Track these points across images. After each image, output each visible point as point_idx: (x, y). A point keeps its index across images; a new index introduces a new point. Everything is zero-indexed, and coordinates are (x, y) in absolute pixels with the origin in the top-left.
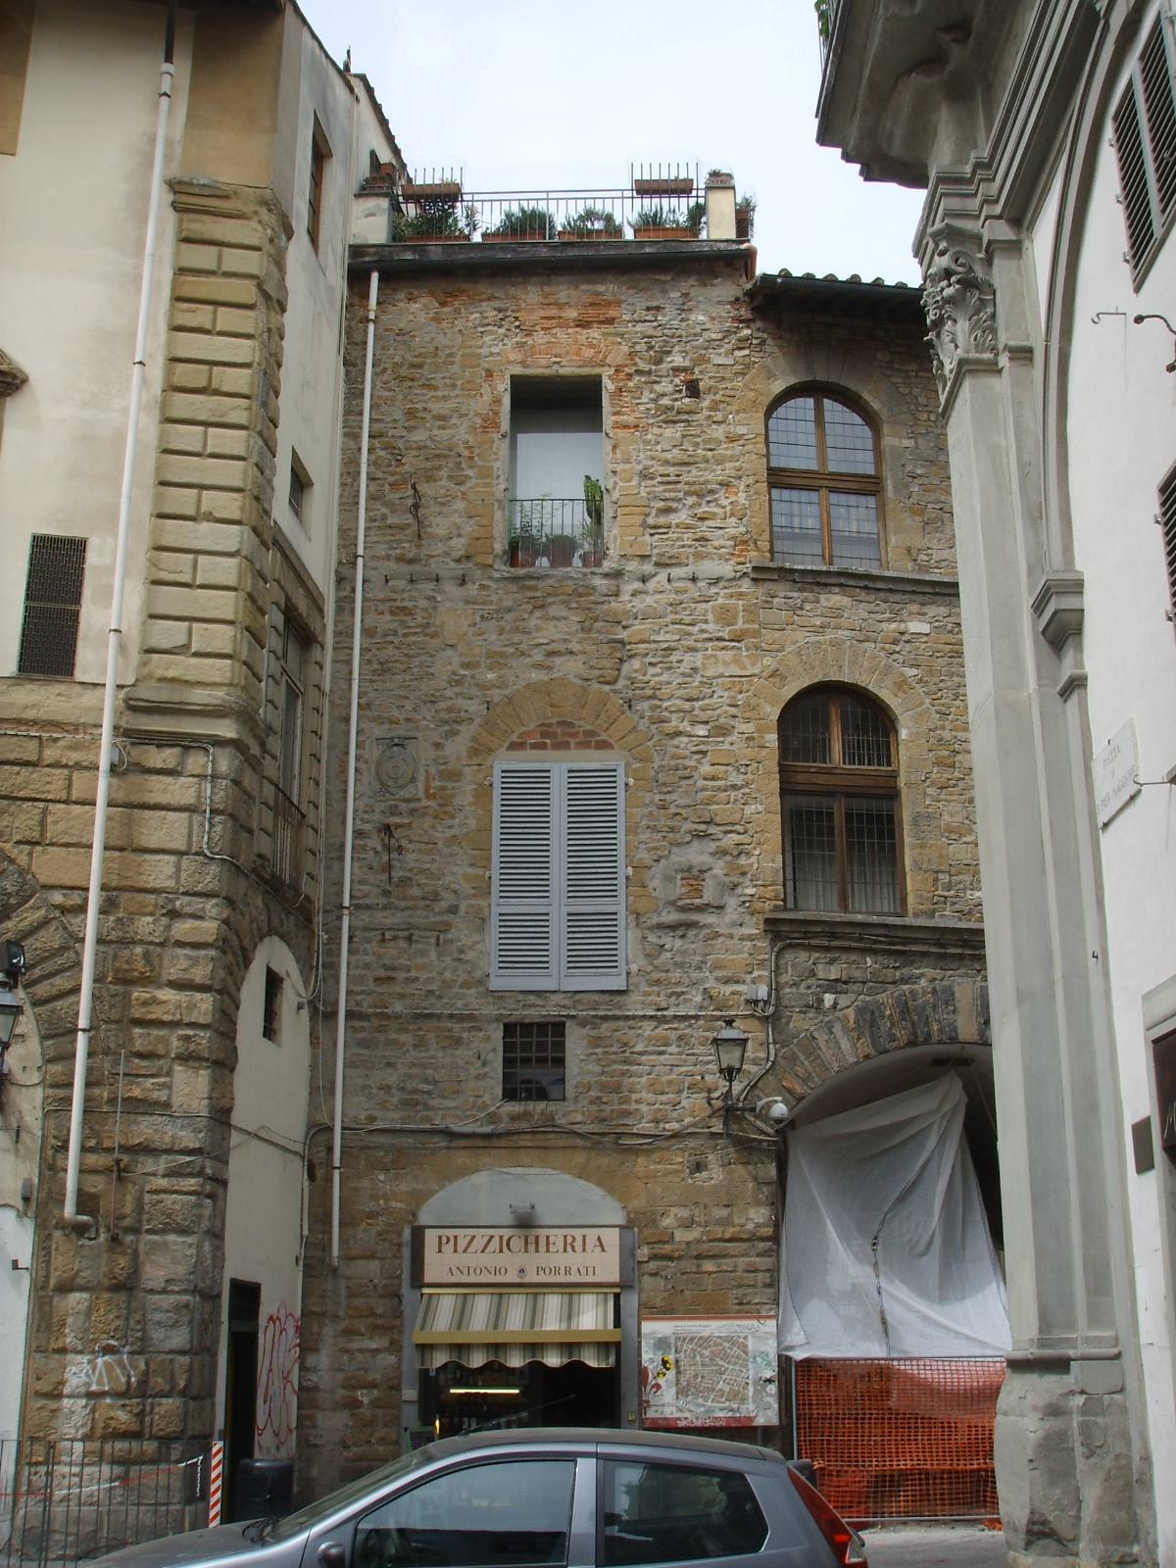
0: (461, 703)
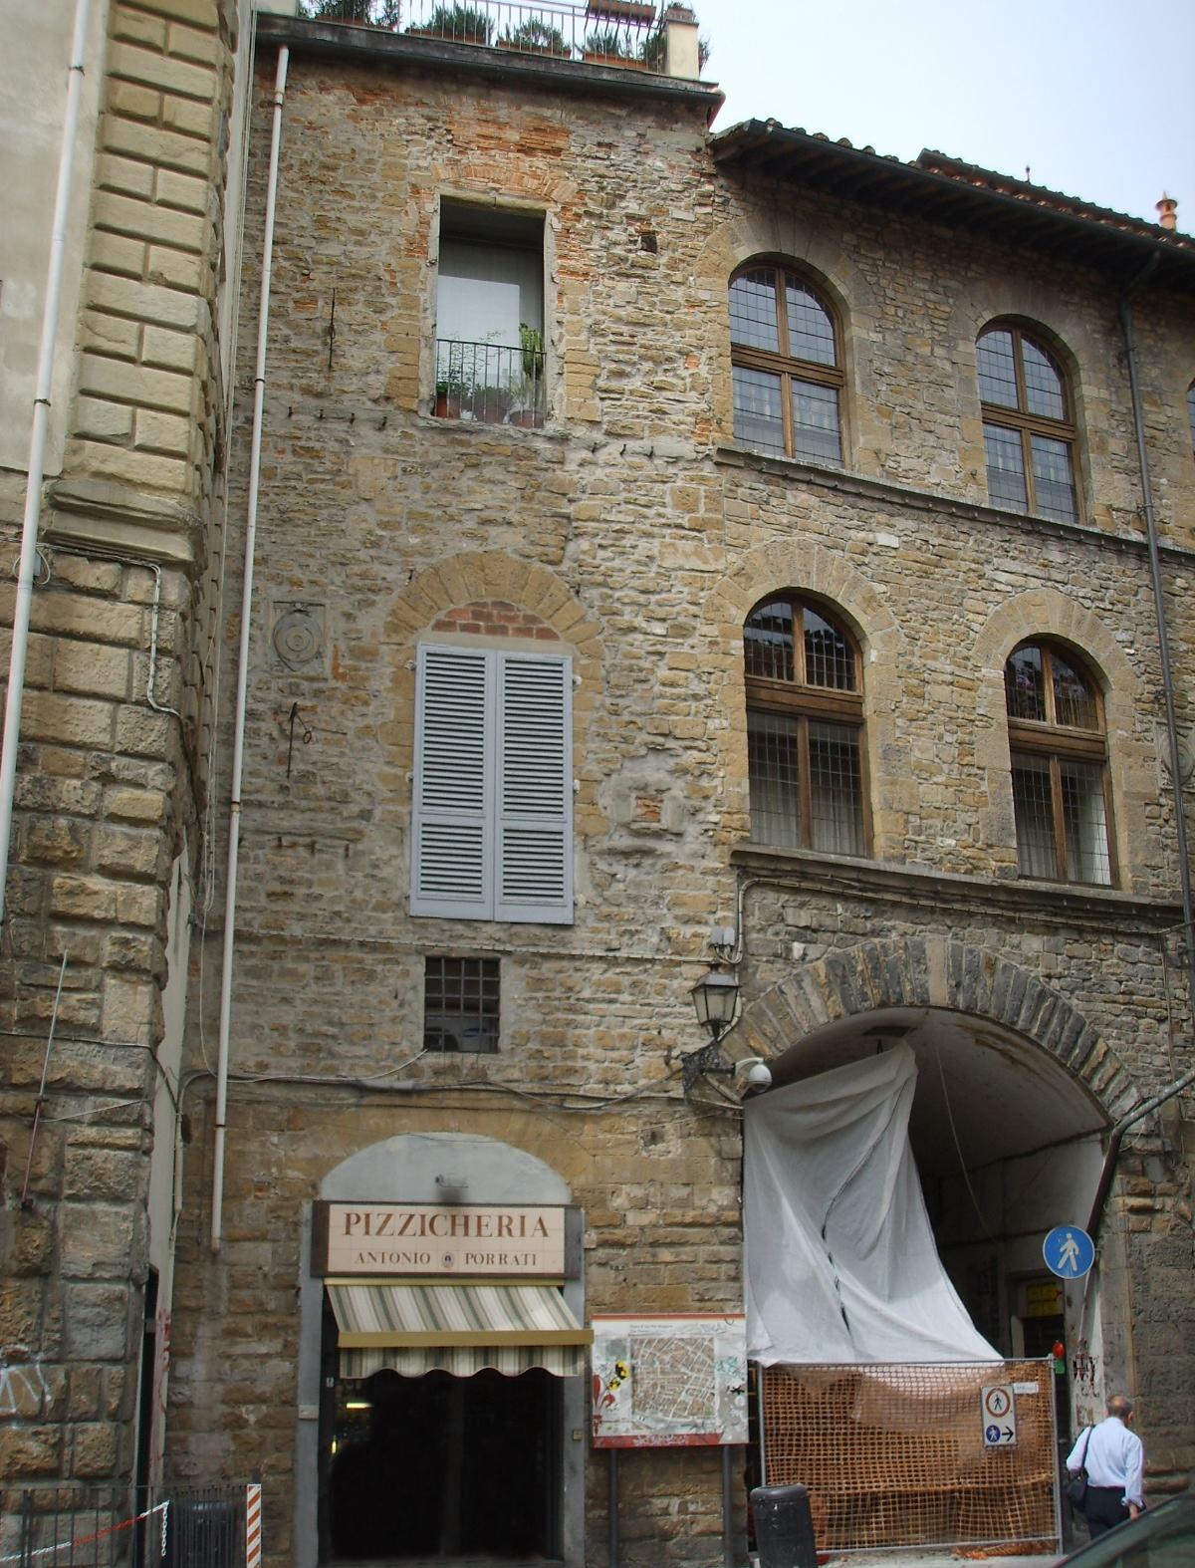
0: (377, 568)
